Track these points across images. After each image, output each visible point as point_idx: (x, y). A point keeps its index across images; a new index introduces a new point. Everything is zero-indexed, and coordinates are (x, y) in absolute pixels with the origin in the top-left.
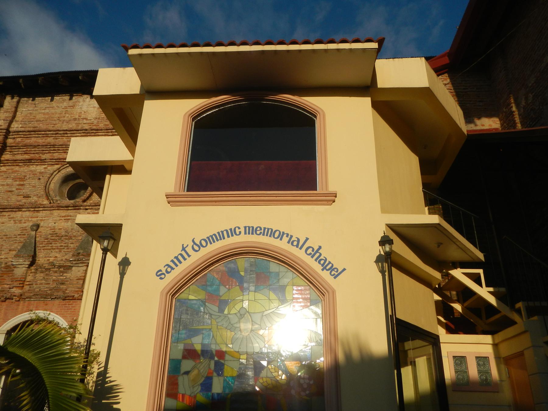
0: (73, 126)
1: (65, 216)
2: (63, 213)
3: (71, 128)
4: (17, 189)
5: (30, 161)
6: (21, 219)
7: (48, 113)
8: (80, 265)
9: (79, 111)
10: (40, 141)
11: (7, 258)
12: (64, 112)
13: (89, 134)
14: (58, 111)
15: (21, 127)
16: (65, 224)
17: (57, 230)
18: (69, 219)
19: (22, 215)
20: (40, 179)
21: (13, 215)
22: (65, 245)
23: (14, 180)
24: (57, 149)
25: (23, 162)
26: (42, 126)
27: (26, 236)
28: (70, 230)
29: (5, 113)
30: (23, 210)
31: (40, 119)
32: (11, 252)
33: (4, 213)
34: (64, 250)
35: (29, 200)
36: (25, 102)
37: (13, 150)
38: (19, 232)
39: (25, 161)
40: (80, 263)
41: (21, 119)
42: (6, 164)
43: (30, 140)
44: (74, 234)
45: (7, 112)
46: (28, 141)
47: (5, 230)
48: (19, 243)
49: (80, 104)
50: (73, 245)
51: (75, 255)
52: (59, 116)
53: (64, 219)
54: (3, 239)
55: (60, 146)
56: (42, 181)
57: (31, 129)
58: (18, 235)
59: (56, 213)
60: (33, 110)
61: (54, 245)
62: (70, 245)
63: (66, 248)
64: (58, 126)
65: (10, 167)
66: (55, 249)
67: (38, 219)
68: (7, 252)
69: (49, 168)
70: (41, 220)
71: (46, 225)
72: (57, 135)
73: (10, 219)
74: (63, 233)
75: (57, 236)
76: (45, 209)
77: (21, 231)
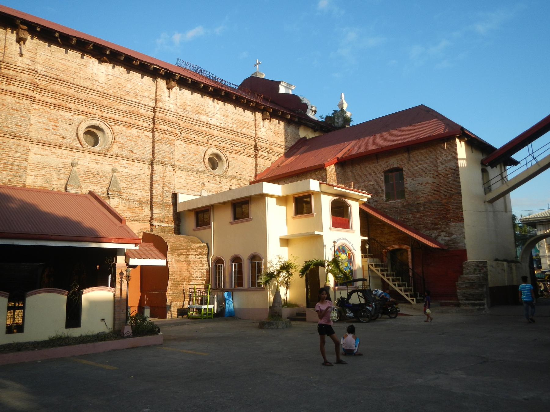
0: (88, 84)
1: (95, 160)
2: (94, 157)
4: (53, 129)
5: (60, 106)
6: (61, 155)
7: (64, 65)
8: (116, 198)
9: (91, 71)
10: (64, 90)
11: (57, 185)
12: (79, 69)
13: (102, 96)
14: (74, 65)
15: (45, 71)
17: (91, 170)
18: (98, 162)
19: (61, 152)
20: (70, 124)
21: (54, 150)
22: (99, 181)
24: (80, 102)
25: (54, 105)
26: (63, 76)
27: (68, 170)
28: (100, 171)
29: (29, 52)
30: (63, 148)
31: (59, 68)
32: (60, 181)
33: (47, 148)
34: (99, 185)
35: (65, 141)
36: (42, 45)
38: (62, 166)
39: (56, 106)
41: (41, 62)
42: (38, 103)
43: (54, 86)
45: (30, 51)
46: (52, 87)
47: (50, 162)
48: (64, 174)
49: (91, 65)
50: (105, 182)
52: (75, 70)
56: (74, 127)
57: (55, 76)
58: (62, 168)
59: (88, 155)
60: (51, 57)
61: (92, 180)
62: (102, 182)
64: (77, 81)
66: (92, 183)
67: (75, 158)
68: (56, 180)
69: (75, 116)
70: (78, 159)
71: (82, 163)
72: (77, 89)
73: (52, 154)
74: (96, 172)
75: (92, 174)
76: (80, 151)
77: (63, 165)
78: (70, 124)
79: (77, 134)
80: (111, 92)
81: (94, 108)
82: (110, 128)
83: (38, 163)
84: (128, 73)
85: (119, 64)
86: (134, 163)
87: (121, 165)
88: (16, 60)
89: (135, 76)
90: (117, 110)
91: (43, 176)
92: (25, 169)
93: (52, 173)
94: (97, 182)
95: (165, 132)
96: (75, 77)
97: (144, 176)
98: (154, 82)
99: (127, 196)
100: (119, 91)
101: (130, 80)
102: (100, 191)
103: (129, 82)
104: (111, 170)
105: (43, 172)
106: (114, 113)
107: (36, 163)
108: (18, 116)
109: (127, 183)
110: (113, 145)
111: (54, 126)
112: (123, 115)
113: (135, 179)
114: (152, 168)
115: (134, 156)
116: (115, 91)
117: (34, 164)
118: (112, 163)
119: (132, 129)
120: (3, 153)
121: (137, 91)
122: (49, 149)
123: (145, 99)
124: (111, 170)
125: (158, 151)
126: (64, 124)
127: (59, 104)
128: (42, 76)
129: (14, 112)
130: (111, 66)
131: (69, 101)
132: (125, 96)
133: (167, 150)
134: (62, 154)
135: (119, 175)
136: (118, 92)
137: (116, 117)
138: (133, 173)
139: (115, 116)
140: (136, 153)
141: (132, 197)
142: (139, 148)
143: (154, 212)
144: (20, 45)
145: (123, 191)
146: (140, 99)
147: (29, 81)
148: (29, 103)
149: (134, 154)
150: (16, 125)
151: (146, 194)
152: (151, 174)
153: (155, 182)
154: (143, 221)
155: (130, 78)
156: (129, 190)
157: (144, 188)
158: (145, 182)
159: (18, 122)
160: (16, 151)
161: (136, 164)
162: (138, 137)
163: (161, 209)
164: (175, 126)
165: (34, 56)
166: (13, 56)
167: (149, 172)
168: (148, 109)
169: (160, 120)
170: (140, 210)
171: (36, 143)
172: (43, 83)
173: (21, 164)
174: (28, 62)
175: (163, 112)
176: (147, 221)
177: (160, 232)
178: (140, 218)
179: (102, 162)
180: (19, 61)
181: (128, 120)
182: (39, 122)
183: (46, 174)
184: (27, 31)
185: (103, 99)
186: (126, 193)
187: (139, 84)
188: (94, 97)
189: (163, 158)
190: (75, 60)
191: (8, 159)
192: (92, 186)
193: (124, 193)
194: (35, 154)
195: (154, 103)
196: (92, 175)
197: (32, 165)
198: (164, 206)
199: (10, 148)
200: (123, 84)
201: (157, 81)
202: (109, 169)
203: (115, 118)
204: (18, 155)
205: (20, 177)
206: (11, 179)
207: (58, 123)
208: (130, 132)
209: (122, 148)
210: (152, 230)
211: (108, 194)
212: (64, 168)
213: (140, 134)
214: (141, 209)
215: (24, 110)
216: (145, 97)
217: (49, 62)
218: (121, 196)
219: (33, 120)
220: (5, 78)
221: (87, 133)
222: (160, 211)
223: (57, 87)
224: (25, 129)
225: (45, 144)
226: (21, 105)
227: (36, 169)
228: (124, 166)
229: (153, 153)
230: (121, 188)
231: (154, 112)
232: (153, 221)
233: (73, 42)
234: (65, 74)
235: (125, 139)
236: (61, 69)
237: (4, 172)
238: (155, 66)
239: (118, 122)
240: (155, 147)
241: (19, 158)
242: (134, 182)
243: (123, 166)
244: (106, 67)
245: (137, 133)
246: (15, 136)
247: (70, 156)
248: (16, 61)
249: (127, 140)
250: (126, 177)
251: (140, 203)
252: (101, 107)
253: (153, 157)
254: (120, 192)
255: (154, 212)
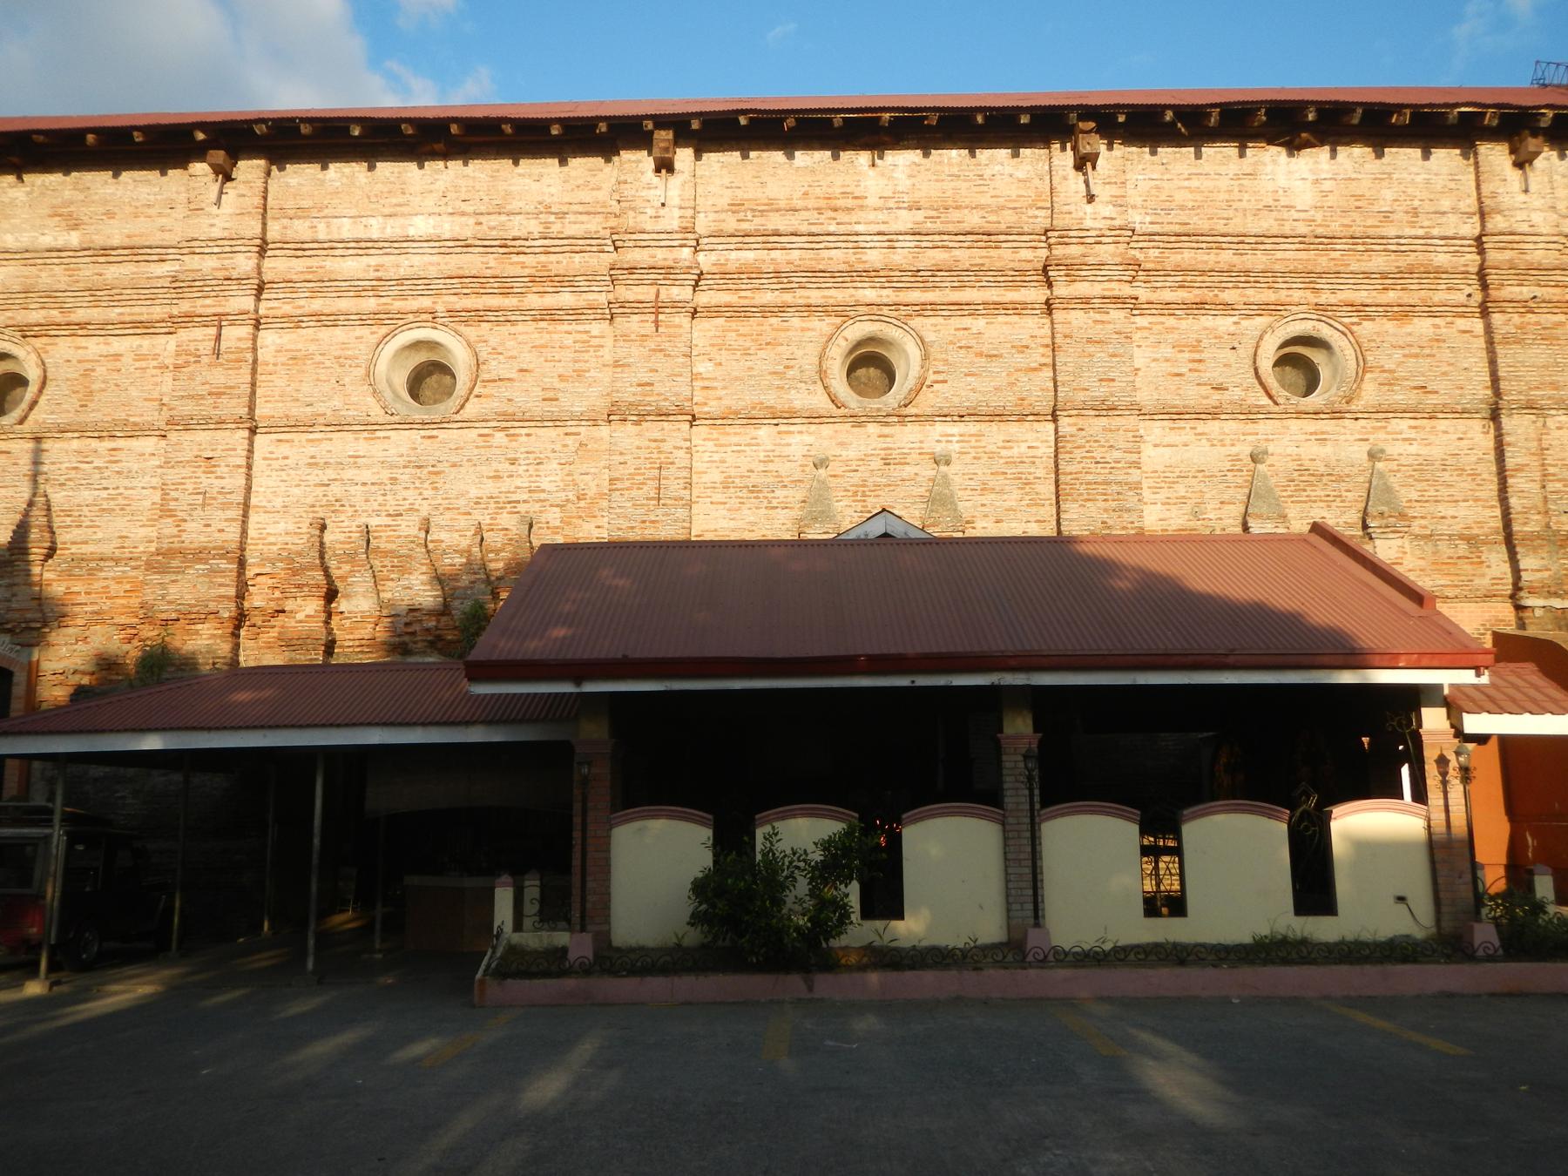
0: (1267, 224)
1: (1316, 433)
2: (1311, 425)
3: (1268, 230)
5: (1200, 305)
6: (1222, 437)
7: (1198, 190)
9: (1270, 186)
10: (1206, 258)
11: (1221, 519)
12: (1236, 189)
14: (1224, 183)
15: (1151, 223)
16: (1321, 448)
17: (1307, 463)
18: (1325, 440)
19: (1222, 428)
21: (1201, 426)
23: (1177, 349)
24: (1252, 279)
25: (1184, 307)
26: (1199, 223)
28: (1334, 463)
29: (1107, 186)
30: (1223, 417)
32: (1226, 507)
33: (1181, 424)
34: (1335, 504)
36: (1135, 157)
37: (1152, 279)
38: (1228, 465)
39: (1190, 306)
40: (1392, 532)
41: (1139, 201)
44: (1347, 471)
45: (1109, 183)
46: (1174, 259)
47: (1195, 461)
49: (1269, 168)
51: (1375, 517)
52: (1227, 197)
53: (1317, 440)
54: (1198, 480)
55: (1261, 274)
56: (1245, 352)
57: (1177, 229)
58: (1228, 470)
59: (1294, 425)
62: (1345, 494)
63: (1338, 499)
64: (1237, 225)
65: (1154, 319)
66: (1315, 501)
67: (1259, 437)
69: (1245, 323)
70: (1267, 440)
71: (1279, 450)
72: (1241, 246)
73: (1199, 437)
74: (1322, 469)
75: (1313, 475)
76: (1271, 416)
78: (1234, 348)
79: (1256, 370)
80: (1335, 228)
81: (1294, 286)
82: (1348, 332)
83: (1167, 469)
84: (1380, 155)
85: (1348, 140)
86: (1433, 422)
87: (1395, 436)
88: (1081, 214)
89: (1404, 158)
90: (1361, 276)
91: (1183, 500)
92: (1135, 488)
93: (1204, 490)
94: (1328, 496)
95: (1527, 306)
96: (1231, 213)
97: (1474, 459)
98: (1468, 159)
99: (1425, 527)
100: (1358, 220)
101: (1390, 174)
102: (1341, 521)
103: (1385, 183)
104: (1365, 456)
105: (1181, 490)
106: (1354, 287)
107: (1160, 468)
108: (1103, 355)
109: (1420, 486)
110: (1362, 380)
111: (1194, 361)
112: (1380, 287)
113: (1444, 470)
114: (1498, 428)
115: (1432, 400)
116: (1346, 222)
117: (1156, 472)
118: (1366, 433)
119: (1416, 320)
120: (1082, 458)
121: (1416, 203)
122: (1188, 426)
123: (1444, 219)
124: (1366, 455)
125: (1512, 369)
126: (1219, 351)
127: (1198, 300)
128: (1147, 238)
129: (1093, 349)
130: (1323, 153)
131: (1223, 285)
132: (1378, 227)
133: (1541, 360)
134: (1225, 434)
135: (1393, 466)
136: (1358, 222)
137: (1362, 296)
138: (1436, 452)
139: (1357, 293)
140: (1437, 392)
141: (1443, 528)
142: (1445, 374)
143: (1522, 567)
144: (1085, 174)
145: (1411, 513)
146: (1426, 223)
147: (1118, 260)
148: (1125, 317)
149: (1431, 396)
150: (1101, 380)
151: (1488, 513)
152: (1496, 449)
153: (1513, 470)
154: (1488, 596)
155: (1389, 169)
156: (1431, 507)
157: (1477, 494)
158: (1480, 475)
159: (1104, 373)
160: (1111, 446)
161: (1442, 425)
162: (1438, 340)
163: (1545, 555)
164: (1559, 278)
165: (1120, 192)
166: (1072, 208)
167: (1489, 442)
168: (1457, 248)
169: (1503, 272)
170: (1472, 563)
171: (1156, 417)
172: (1151, 256)
173: (1126, 477)
174: (1108, 211)
175: (1510, 246)
176: (1502, 596)
177: (1550, 627)
178: (1478, 590)
179: (1335, 437)
180: (1088, 217)
181: (1399, 298)
182: (1155, 360)
183: (1189, 495)
184: (1096, 133)
185: (1316, 255)
186: (1422, 517)
187: (1419, 179)
188: (1288, 255)
189: (1530, 389)
190: (1222, 170)
191: (1094, 470)
192: (1317, 510)
193: (1415, 517)
194: (1156, 446)
195: (1478, 225)
196: (1312, 478)
197: (1152, 475)
198: (1554, 544)
199: (1096, 441)
200: (1368, 194)
201: (1476, 154)
202: (1359, 453)
203: (1359, 301)
204: (1117, 454)
205: (1128, 510)
206: (1108, 520)
207: (1202, 352)
208: (1409, 330)
209: (1391, 384)
210: (1522, 624)
211: (1365, 527)
212: (1232, 470)
213: (1444, 330)
214: (1476, 560)
215: (1117, 336)
216: (1444, 213)
217: (1157, 197)
218: (1406, 529)
219: (1140, 358)
220: (1061, 268)
221: (1282, 361)
222: (1545, 562)
223: (1186, 257)
224: (1125, 384)
225: (1176, 415)
226: (1106, 326)
227: (1163, 485)
228: (1404, 436)
229: (1495, 380)
230: (1404, 504)
231: (1481, 251)
232: (1522, 594)
233: (1213, 120)
234: (1202, 216)
235: (1398, 355)
236: (1190, 204)
237: (1089, 504)
238: (1463, 109)
239: (1367, 309)
240: (1499, 360)
241: (1119, 462)
242: (1443, 479)
243: (1399, 436)
244: (1311, 161)
245: (1432, 330)
246: (1105, 408)
247: (1244, 434)
248: (1081, 219)
249: (1405, 356)
250: (1415, 470)
251: (1471, 540)
252: (1310, 278)
253: (1497, 392)
254: (1402, 516)
255: (1522, 566)
